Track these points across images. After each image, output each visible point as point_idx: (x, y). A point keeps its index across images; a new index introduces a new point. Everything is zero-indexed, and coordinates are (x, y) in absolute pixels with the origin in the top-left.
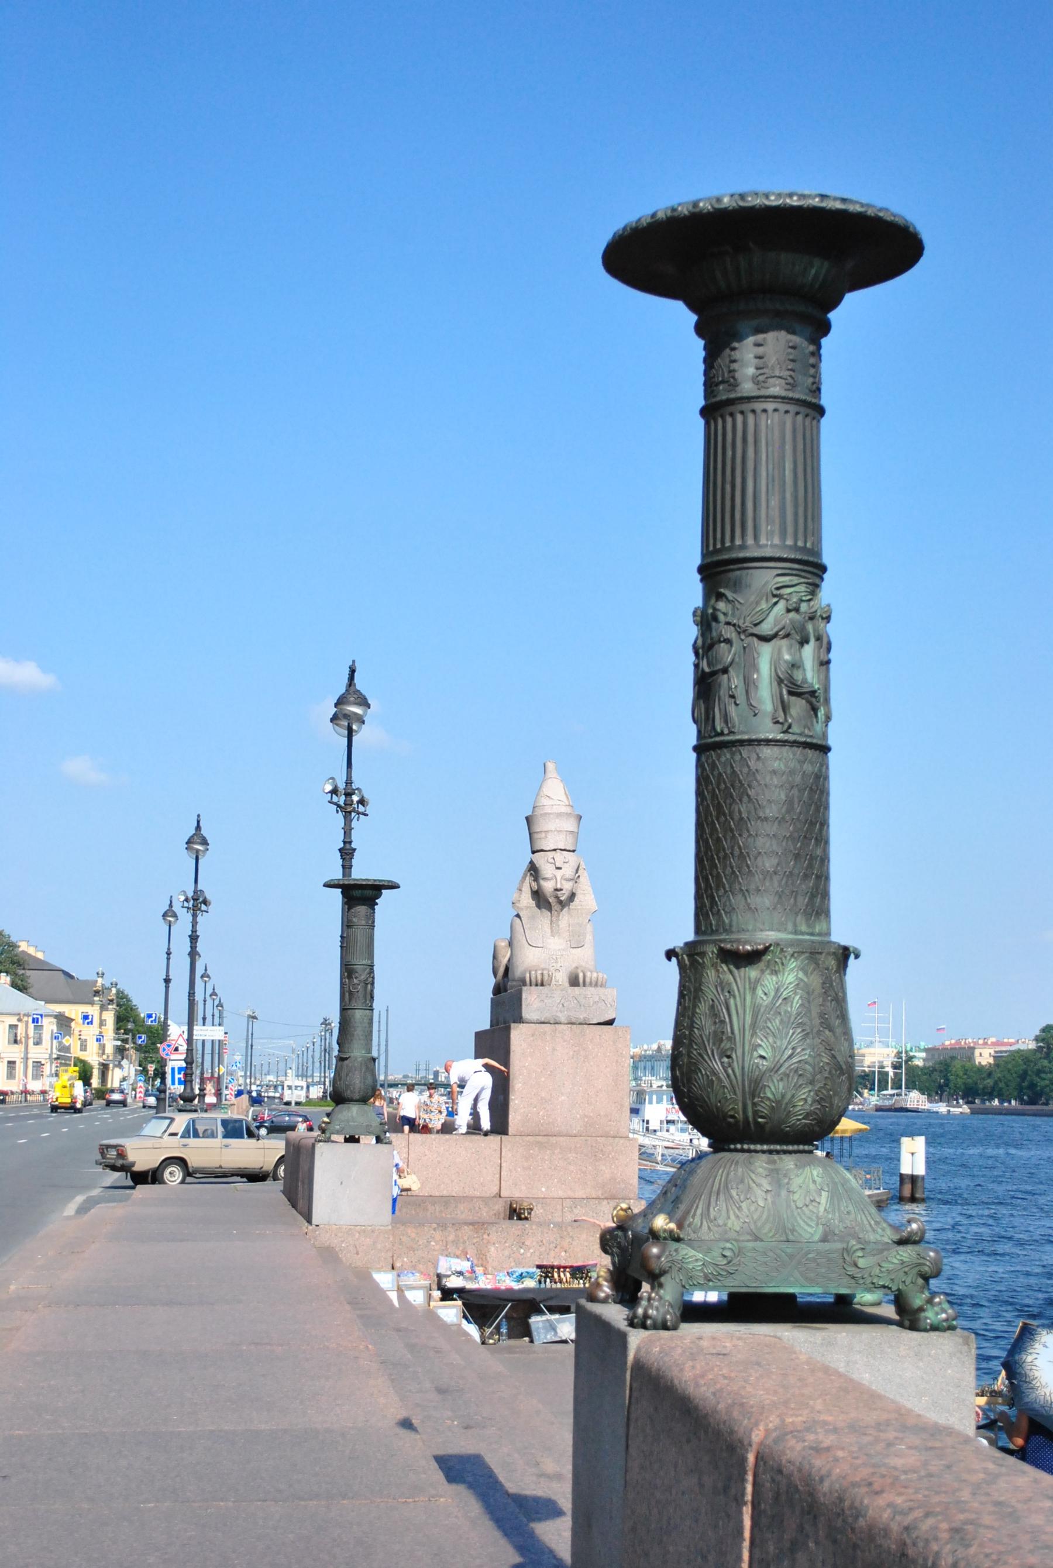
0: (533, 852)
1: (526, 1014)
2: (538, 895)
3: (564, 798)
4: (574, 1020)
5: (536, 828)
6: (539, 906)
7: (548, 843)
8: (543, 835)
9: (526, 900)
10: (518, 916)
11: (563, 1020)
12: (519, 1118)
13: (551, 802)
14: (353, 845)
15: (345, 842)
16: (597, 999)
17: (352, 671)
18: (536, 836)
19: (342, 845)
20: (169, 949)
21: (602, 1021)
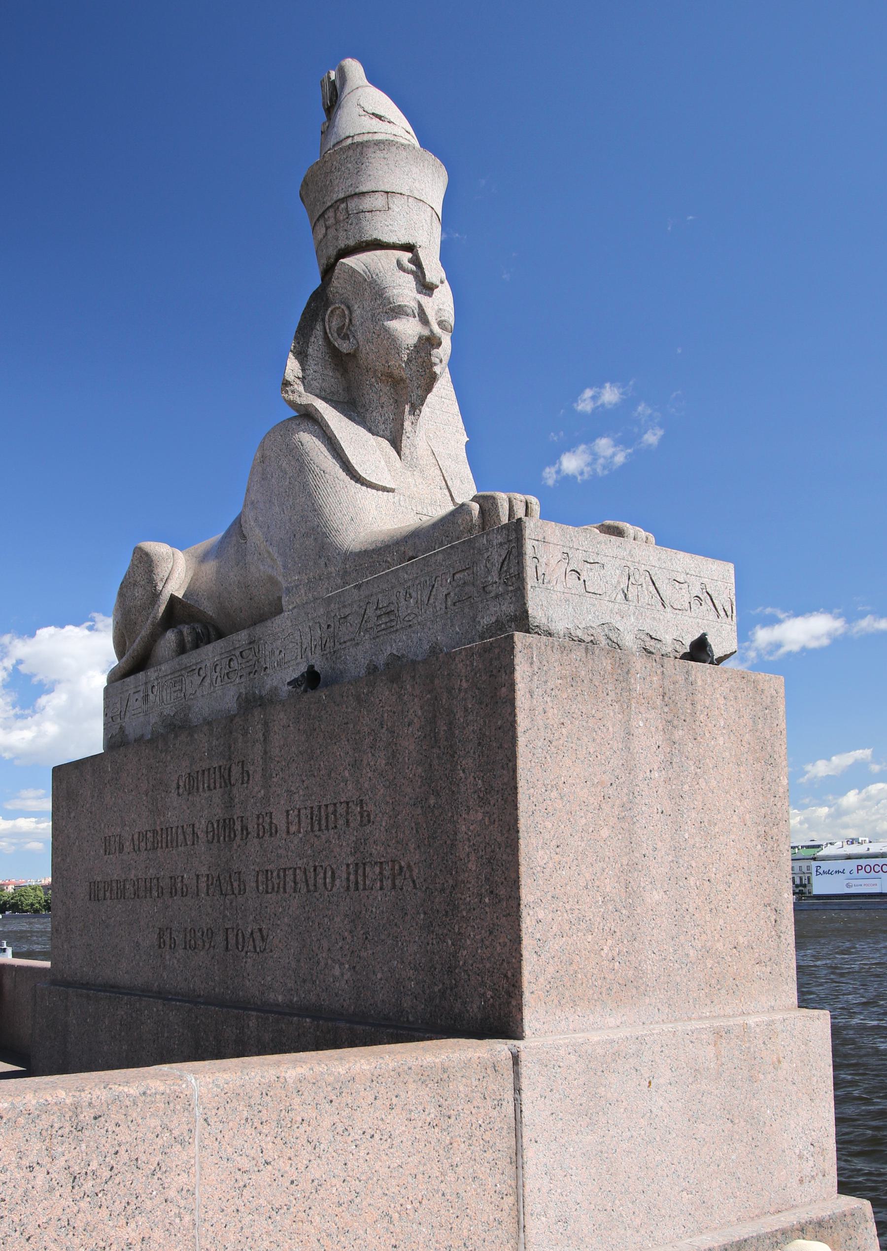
1: (540, 604)
11: (629, 640)
12: (551, 969)
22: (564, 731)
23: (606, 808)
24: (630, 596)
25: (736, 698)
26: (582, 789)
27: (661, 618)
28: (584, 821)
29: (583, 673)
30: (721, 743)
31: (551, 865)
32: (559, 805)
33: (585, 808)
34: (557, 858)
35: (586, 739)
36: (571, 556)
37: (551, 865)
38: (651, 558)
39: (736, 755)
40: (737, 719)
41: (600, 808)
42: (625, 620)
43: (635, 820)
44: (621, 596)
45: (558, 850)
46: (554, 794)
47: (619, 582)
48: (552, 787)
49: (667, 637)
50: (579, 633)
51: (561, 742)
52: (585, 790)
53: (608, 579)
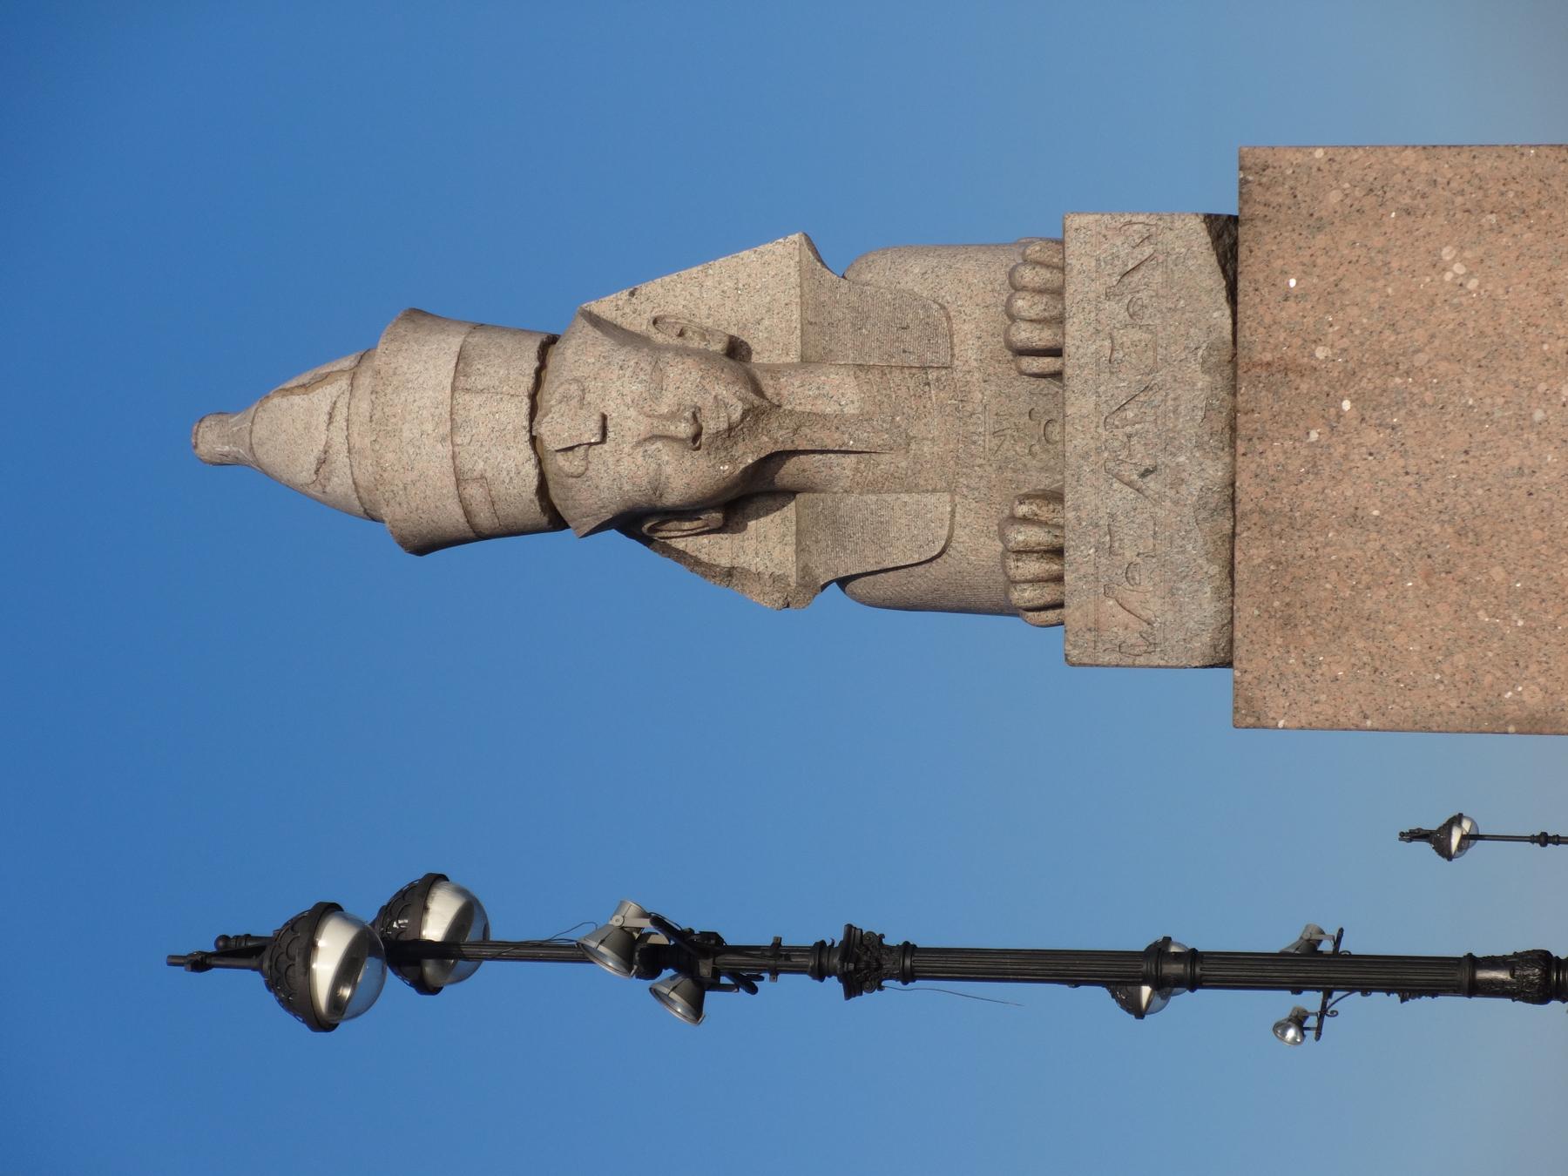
0: (557, 522)
2: (739, 501)
3: (322, 398)
4: (1219, 423)
5: (451, 516)
6: (790, 493)
7: (510, 472)
8: (474, 492)
9: (766, 543)
10: (843, 582)
11: (1216, 472)
13: (340, 459)
14: (836, 936)
15: (820, 974)
16: (1116, 309)
17: (200, 963)
18: (484, 518)
19: (833, 985)
20: (1533, 839)
21: (1217, 283)
22: (1360, 644)
23: (1464, 568)
24: (1148, 463)
25: (1284, 273)
26: (1437, 615)
27: (1172, 395)
28: (1481, 613)
29: (1276, 604)
30: (1355, 311)
31: (1542, 680)
32: (1460, 659)
33: (1465, 610)
34: (1533, 668)
35: (1369, 604)
36: (1104, 581)
37: (1542, 680)
38: (1084, 411)
39: (1375, 280)
40: (1317, 271)
41: (1462, 581)
42: (1184, 475)
43: (1478, 512)
44: (1152, 484)
45: (1522, 664)
46: (1446, 667)
47: (1130, 484)
48: (1436, 671)
49: (1200, 385)
50: (1214, 569)
51: (1374, 650)
52: (1439, 607)
53: (1129, 507)
